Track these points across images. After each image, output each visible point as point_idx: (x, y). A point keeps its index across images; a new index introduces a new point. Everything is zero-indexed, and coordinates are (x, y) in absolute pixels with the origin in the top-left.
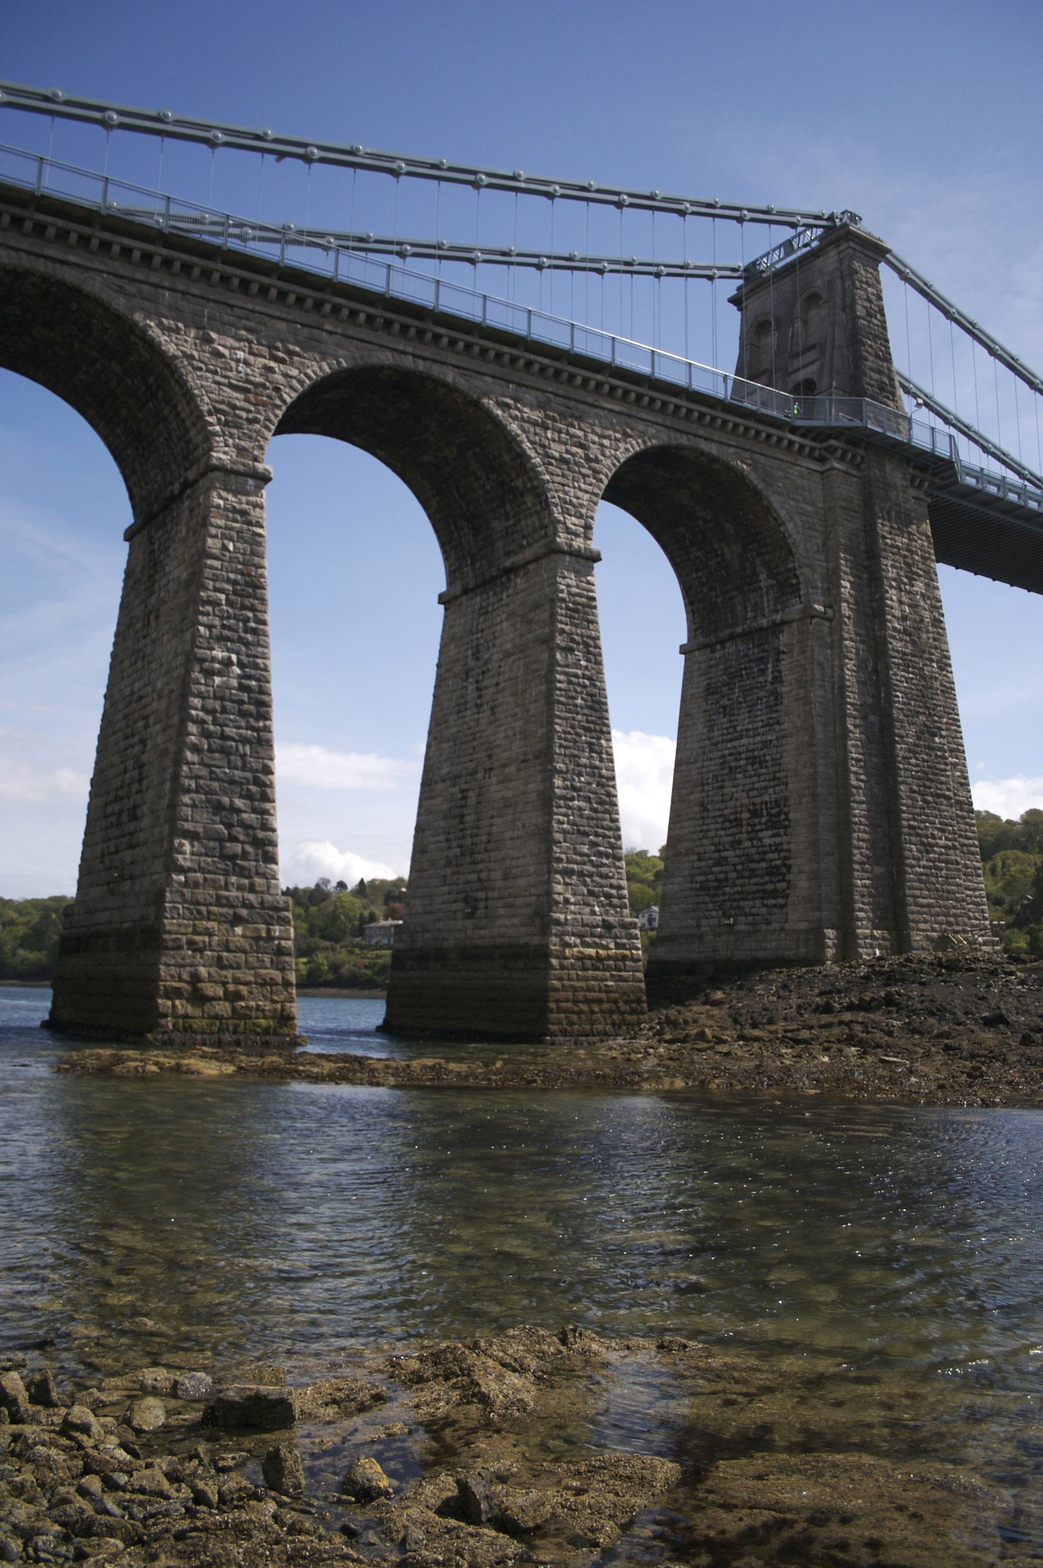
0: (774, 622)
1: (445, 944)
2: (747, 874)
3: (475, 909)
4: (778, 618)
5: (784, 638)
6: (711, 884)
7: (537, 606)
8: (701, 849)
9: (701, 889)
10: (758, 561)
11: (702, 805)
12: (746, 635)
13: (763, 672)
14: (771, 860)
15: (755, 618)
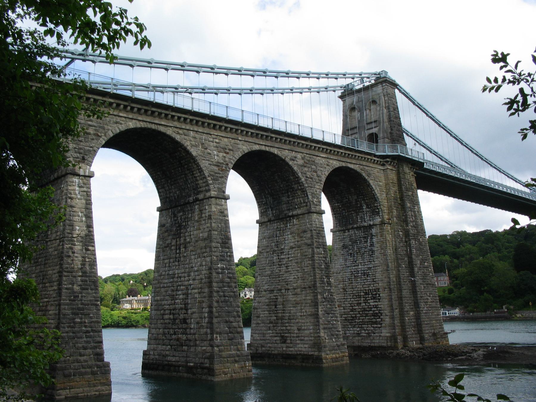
0: (370, 225)
2: (365, 315)
3: (286, 340)
4: (372, 223)
5: (374, 231)
6: (350, 318)
7: (305, 232)
8: (344, 305)
9: (346, 320)
12: (359, 228)
13: (366, 242)
14: (374, 311)
15: (362, 221)
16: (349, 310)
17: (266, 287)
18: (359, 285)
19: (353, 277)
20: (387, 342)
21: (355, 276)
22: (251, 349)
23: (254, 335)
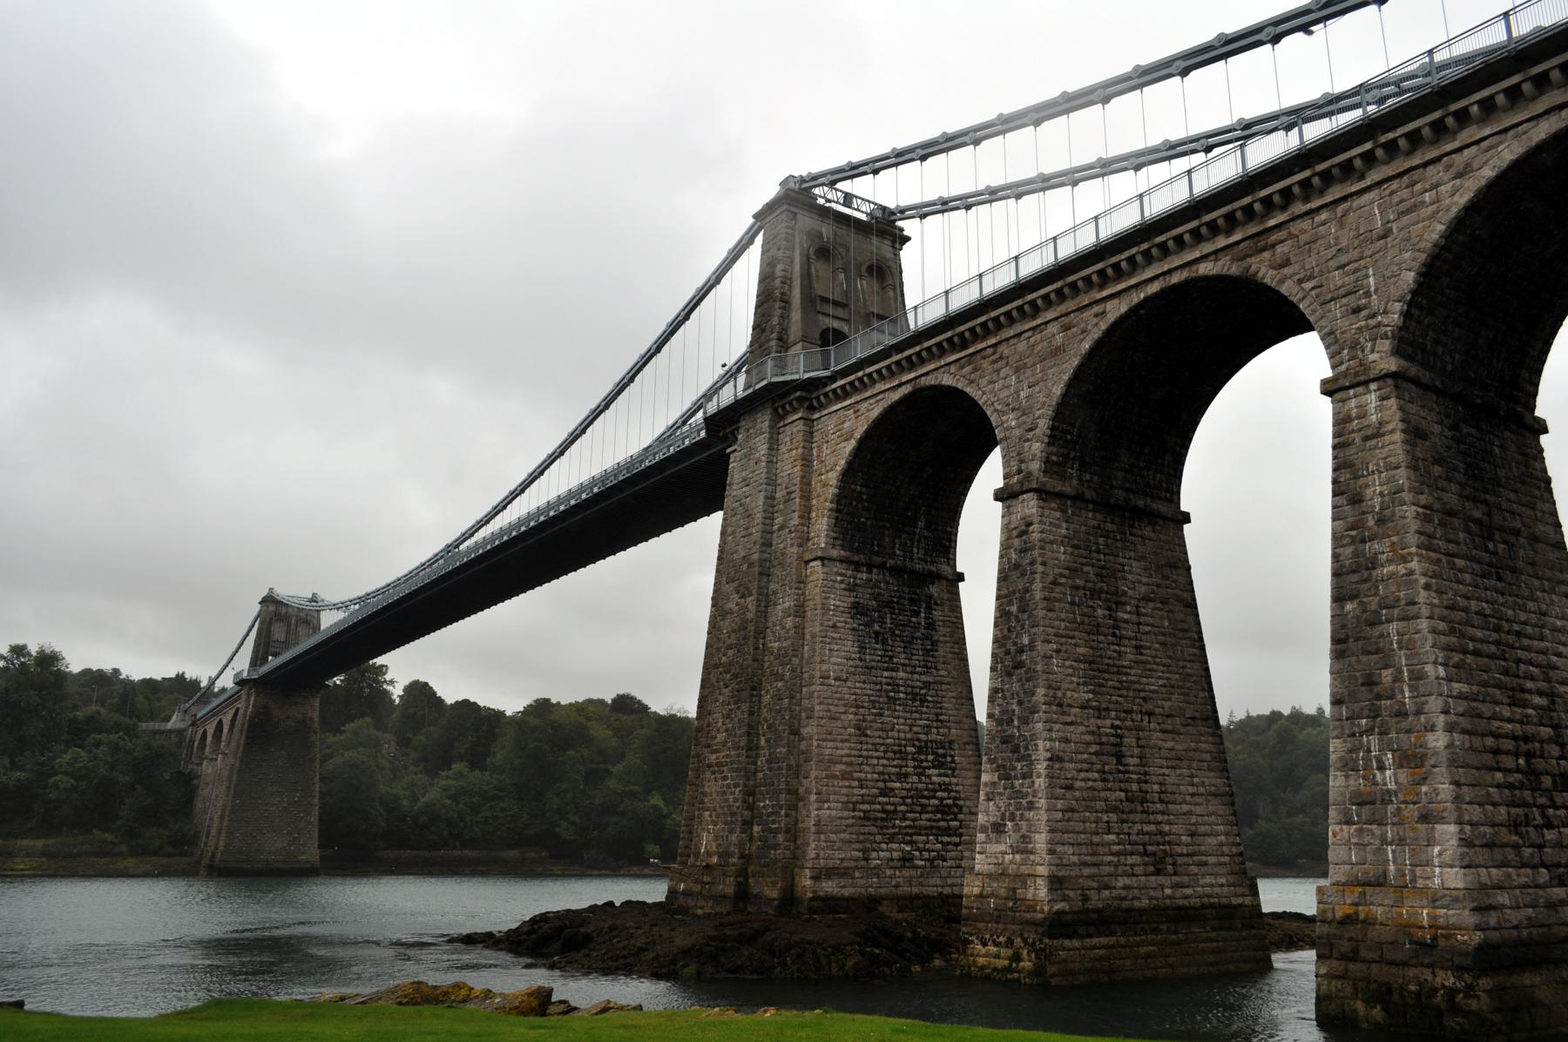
1: (1136, 904)
11: (858, 728)
13: (916, 614)
14: (942, 799)
22: (1065, 898)
23: (1059, 848)
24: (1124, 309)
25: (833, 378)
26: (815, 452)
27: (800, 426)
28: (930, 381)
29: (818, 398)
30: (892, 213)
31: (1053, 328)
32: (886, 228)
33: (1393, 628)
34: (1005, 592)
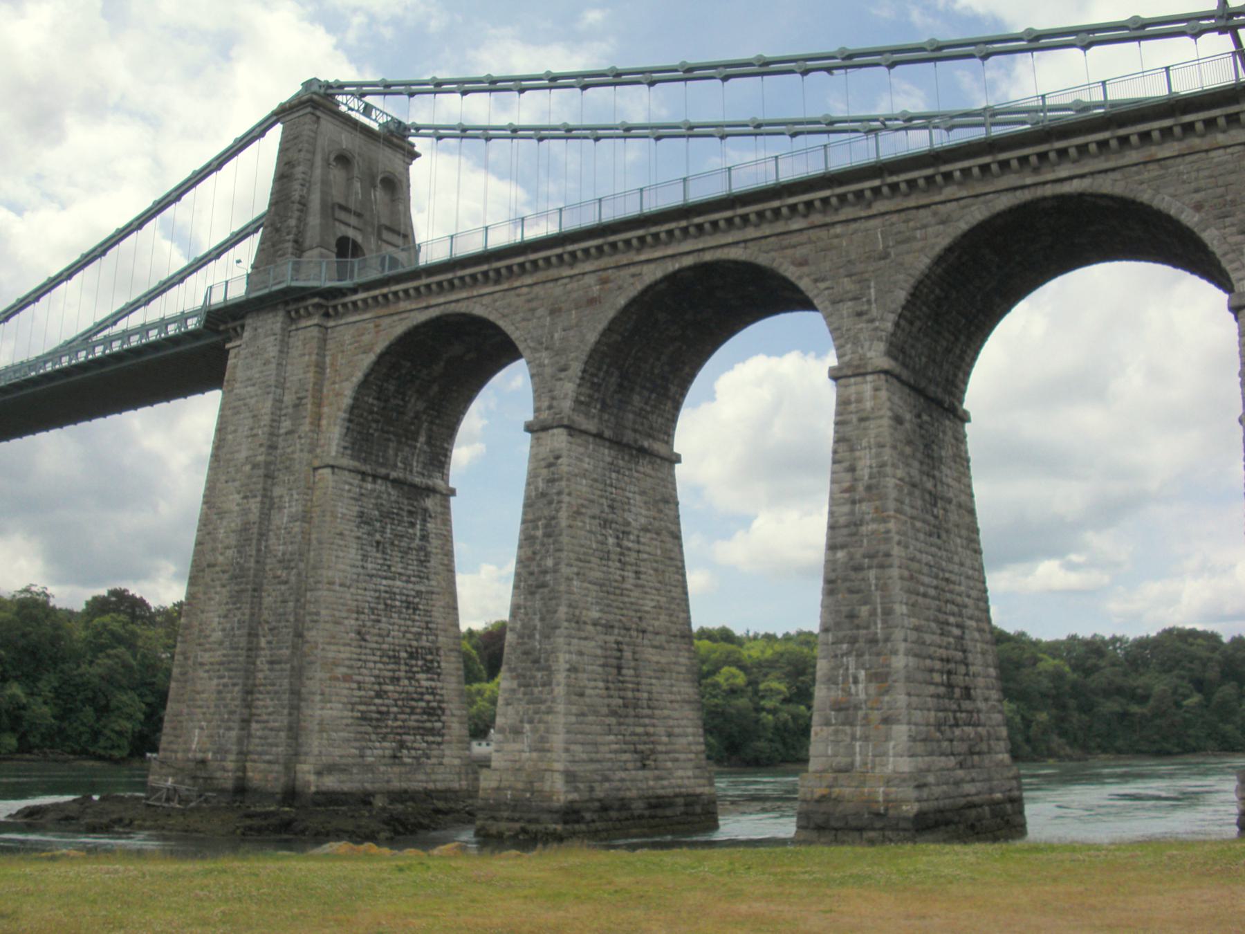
1: (628, 794)
2: (408, 710)
8: (360, 678)
9: (363, 718)
10: (425, 425)
11: (359, 633)
13: (413, 525)
14: (428, 702)
16: (372, 693)
17: (595, 614)
18: (396, 630)
19: (382, 606)
20: (460, 780)
21: (386, 604)
22: (576, 789)
23: (573, 747)
24: (659, 274)
25: (354, 290)
26: (328, 360)
27: (315, 332)
28: (462, 308)
29: (335, 307)
30: (407, 128)
31: (590, 280)
32: (397, 139)
33: (872, 574)
34: (530, 517)
